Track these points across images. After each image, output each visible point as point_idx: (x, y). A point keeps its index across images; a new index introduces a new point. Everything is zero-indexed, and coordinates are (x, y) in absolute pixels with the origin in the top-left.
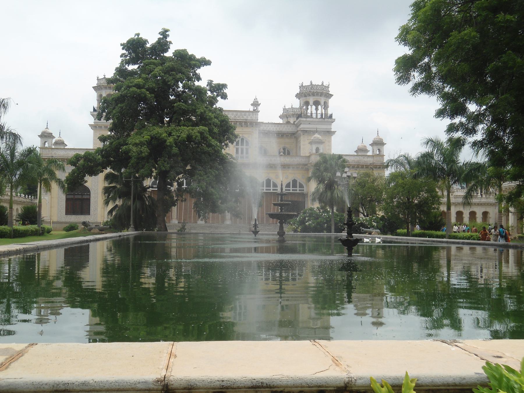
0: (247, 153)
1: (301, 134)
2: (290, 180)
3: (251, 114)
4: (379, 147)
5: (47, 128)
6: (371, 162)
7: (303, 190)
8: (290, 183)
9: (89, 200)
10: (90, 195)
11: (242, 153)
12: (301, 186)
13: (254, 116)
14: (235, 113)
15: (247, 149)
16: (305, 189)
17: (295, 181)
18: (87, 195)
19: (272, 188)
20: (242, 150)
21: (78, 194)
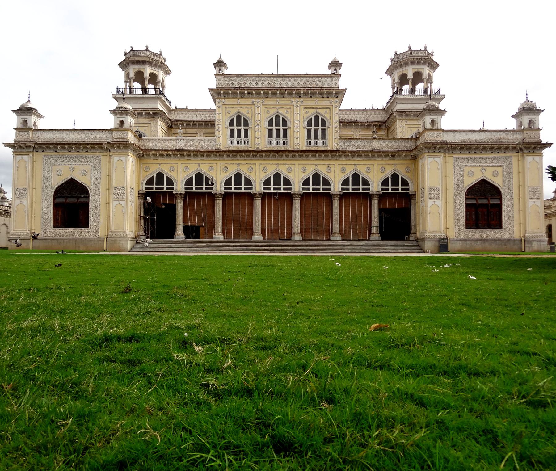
0: (324, 136)
1: (397, 117)
2: (388, 173)
3: (329, 79)
4: (531, 117)
5: (29, 101)
6: (520, 141)
7: (408, 189)
8: (388, 178)
9: (87, 205)
10: (88, 197)
11: (316, 136)
12: (405, 183)
13: (333, 82)
14: (305, 79)
15: (323, 131)
16: (410, 187)
17: (395, 177)
18: (85, 197)
19: (361, 187)
20: (316, 132)
21: (71, 197)
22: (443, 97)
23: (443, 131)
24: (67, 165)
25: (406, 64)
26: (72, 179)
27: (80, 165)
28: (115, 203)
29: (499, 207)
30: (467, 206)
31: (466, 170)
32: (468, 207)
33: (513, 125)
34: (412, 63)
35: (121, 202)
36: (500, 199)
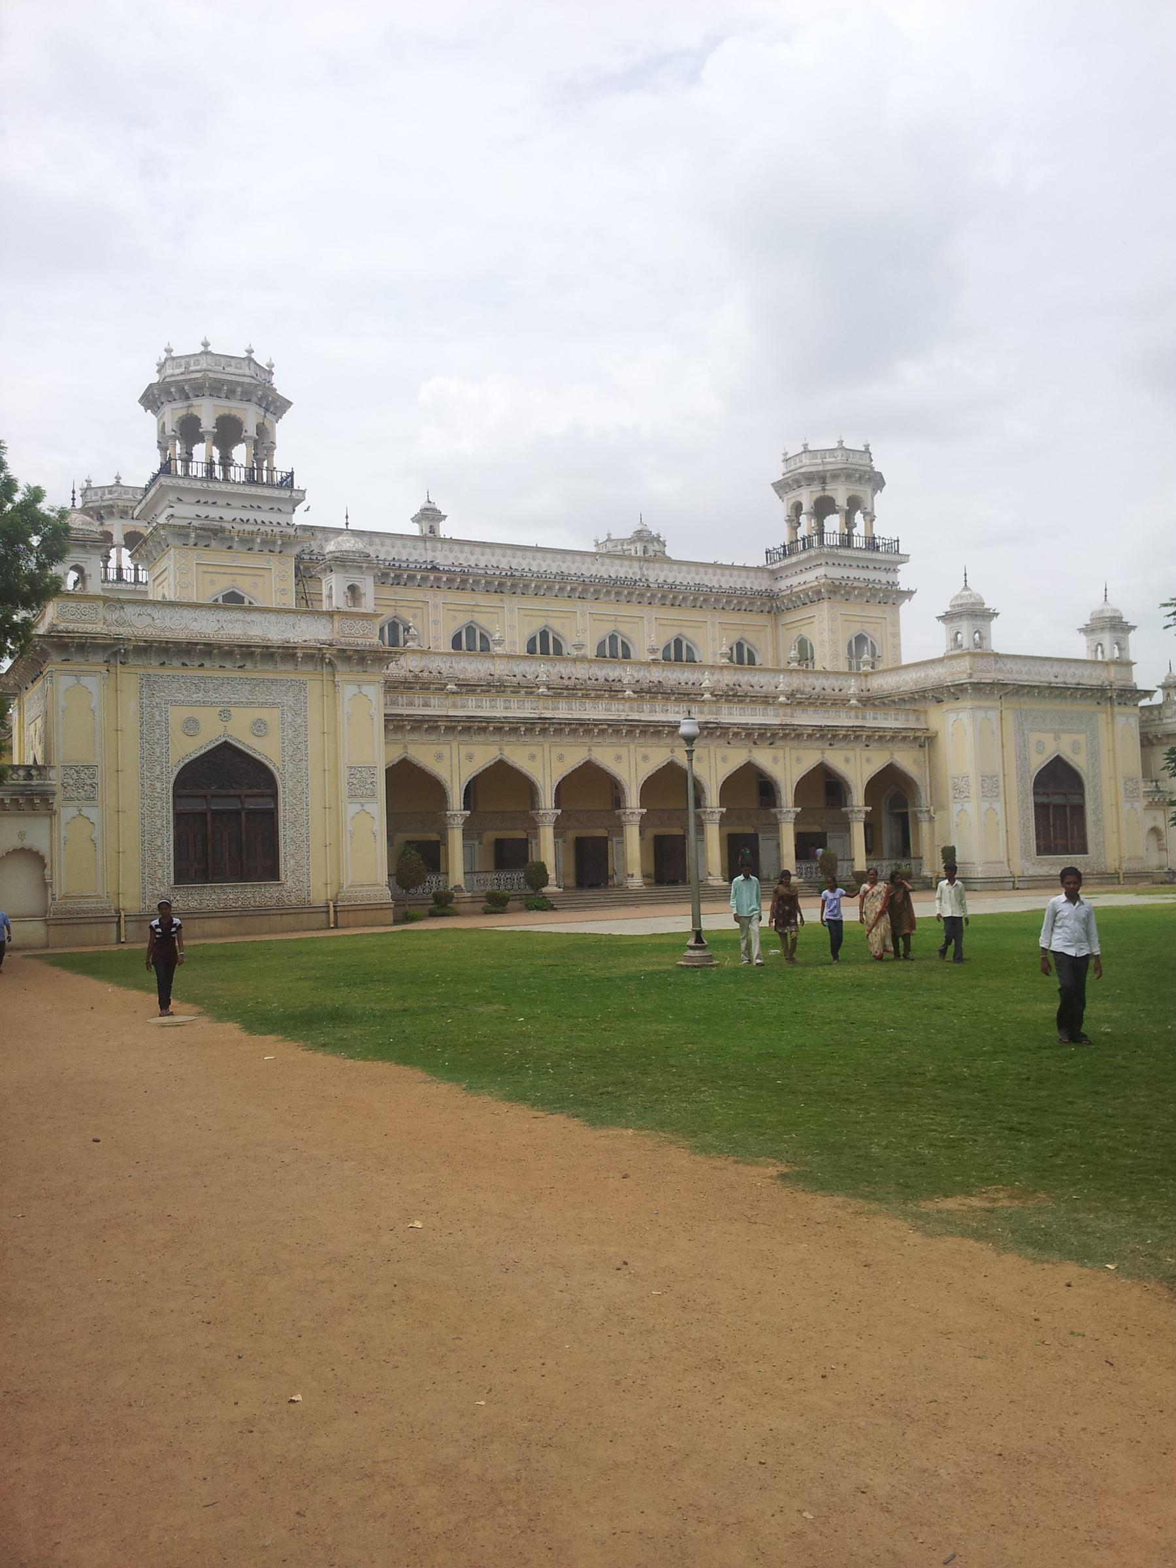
10: (274, 796)
22: (905, 559)
23: (997, 655)
24: (212, 704)
25: (835, 476)
26: (226, 742)
27: (250, 704)
28: (352, 809)
29: (1080, 810)
30: (1037, 805)
31: (1034, 737)
32: (1041, 810)
33: (1079, 648)
34: (849, 477)
35: (368, 807)
36: (1082, 794)
